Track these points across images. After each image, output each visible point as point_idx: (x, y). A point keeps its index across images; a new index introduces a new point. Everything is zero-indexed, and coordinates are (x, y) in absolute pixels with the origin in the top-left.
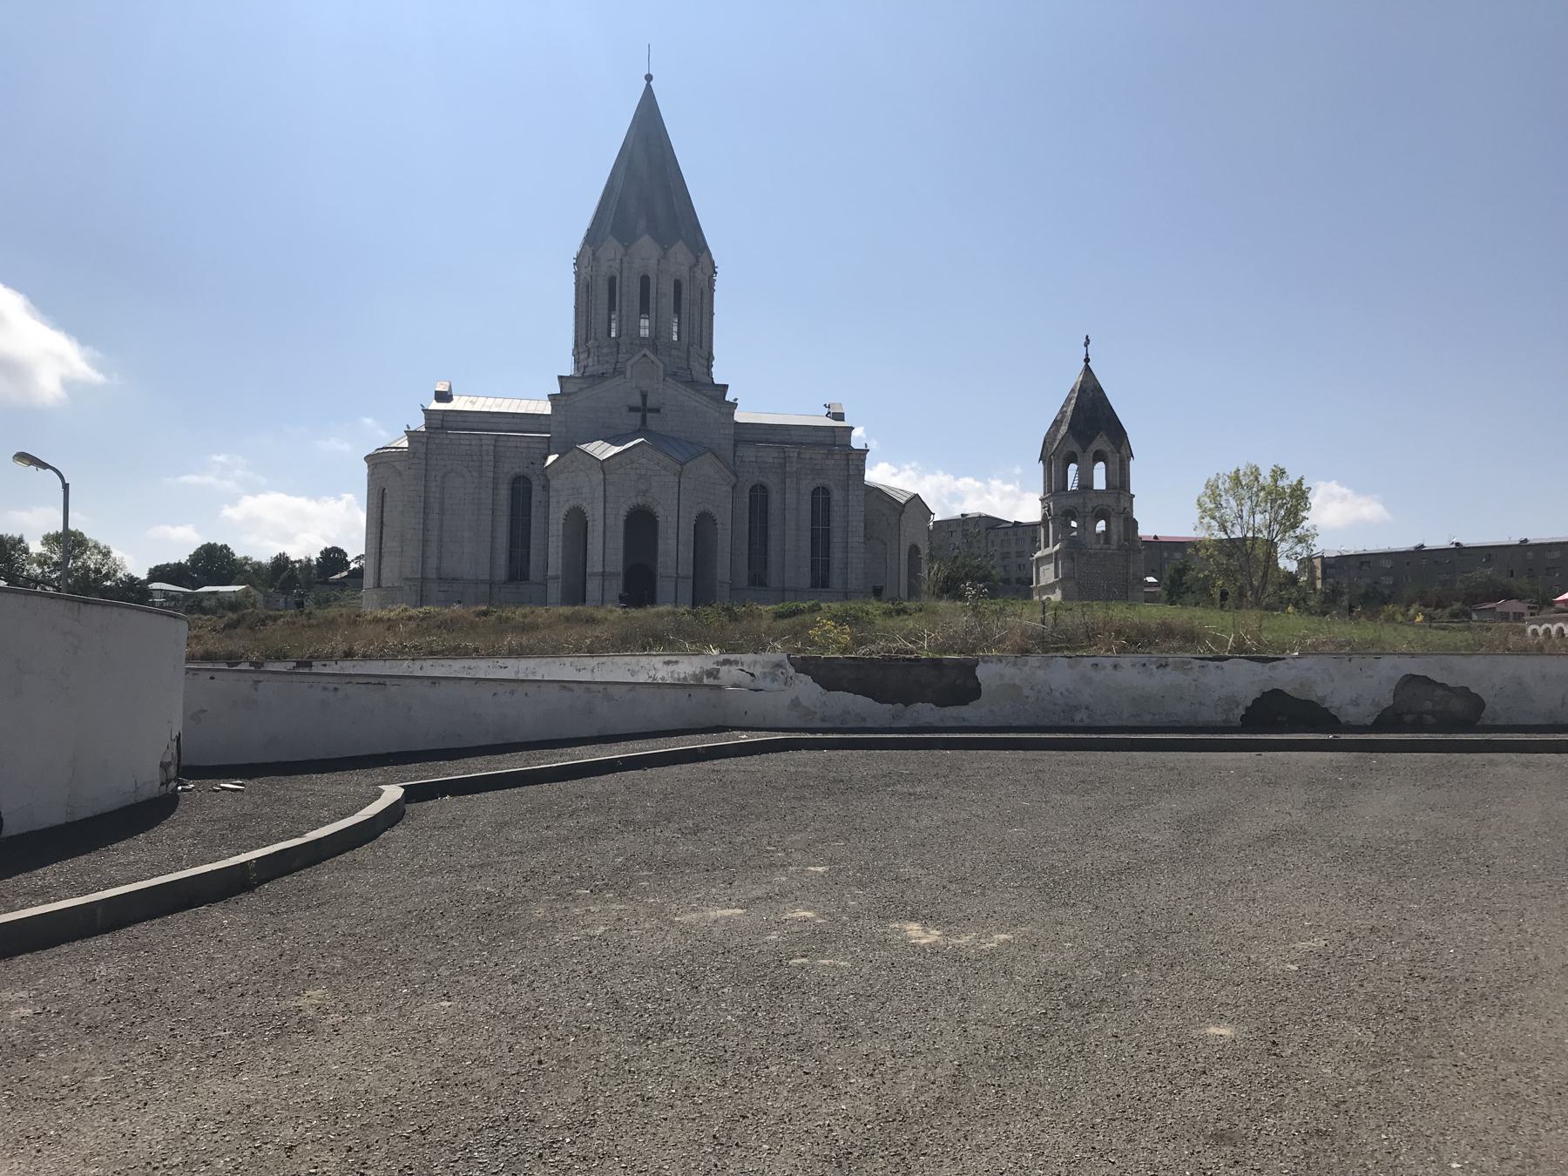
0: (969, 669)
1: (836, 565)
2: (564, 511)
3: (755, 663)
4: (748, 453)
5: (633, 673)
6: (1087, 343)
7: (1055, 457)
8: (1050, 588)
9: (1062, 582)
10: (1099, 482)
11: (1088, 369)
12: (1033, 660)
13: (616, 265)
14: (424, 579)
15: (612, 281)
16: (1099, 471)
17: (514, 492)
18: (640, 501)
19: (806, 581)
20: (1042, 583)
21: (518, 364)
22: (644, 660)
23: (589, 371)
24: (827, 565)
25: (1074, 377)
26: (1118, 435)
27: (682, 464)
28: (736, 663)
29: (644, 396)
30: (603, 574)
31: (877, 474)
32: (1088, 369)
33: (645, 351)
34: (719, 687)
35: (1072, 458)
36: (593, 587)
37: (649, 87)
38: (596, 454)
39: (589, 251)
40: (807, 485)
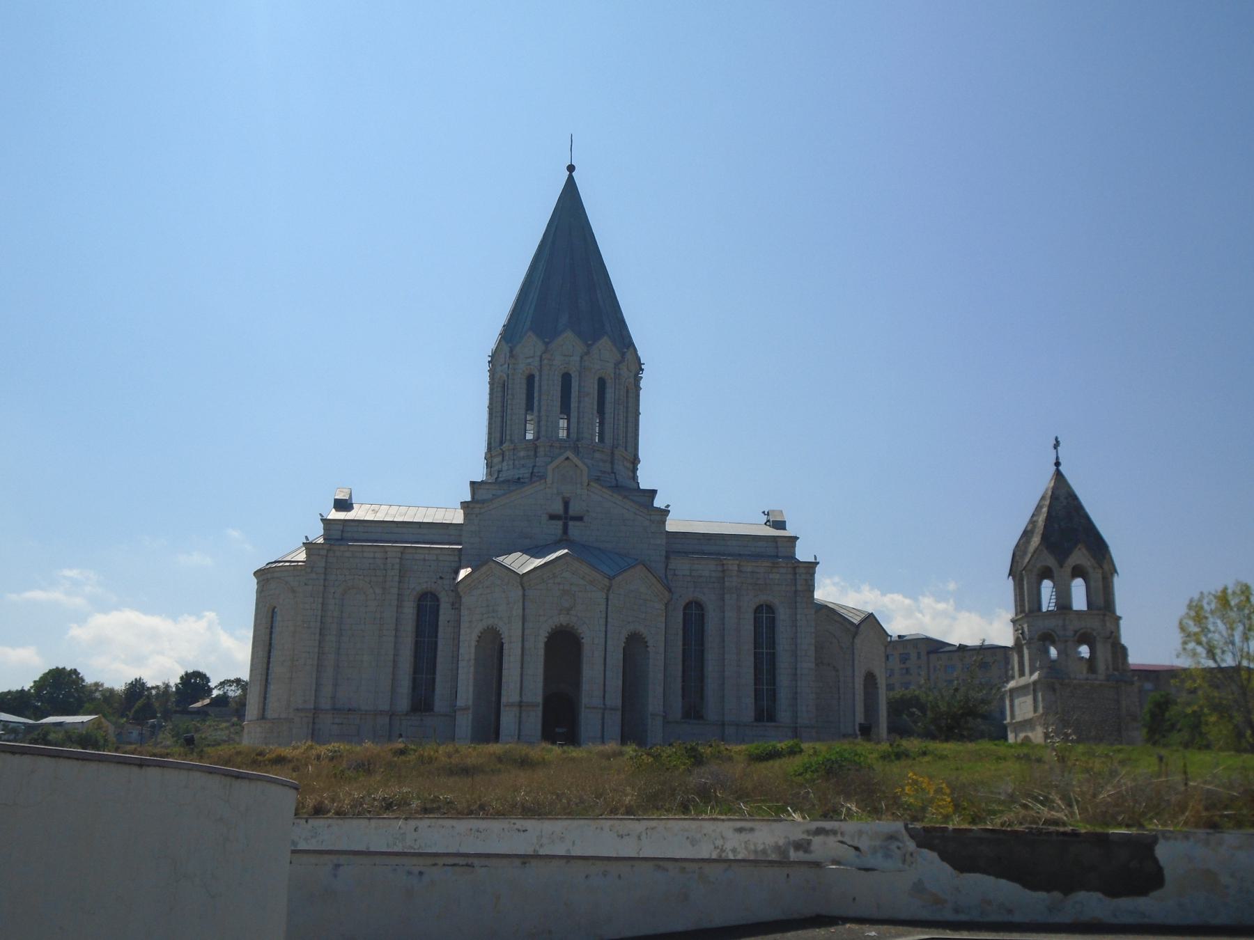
0: (1145, 847)
1: (783, 695)
3: (860, 833)
4: (681, 566)
5: (694, 842)
6: (1057, 445)
7: (1025, 572)
8: (1027, 724)
10: (1079, 601)
11: (1059, 475)
12: (1231, 837)
13: (537, 363)
14: (317, 710)
15: (530, 379)
18: (563, 620)
19: (749, 714)
20: (1018, 719)
22: (708, 827)
23: (503, 476)
25: (1044, 482)
26: (1098, 547)
27: (611, 578)
28: (834, 832)
29: (566, 504)
30: (520, 705)
31: (826, 591)
32: (1059, 475)
33: (569, 454)
34: (817, 865)
35: (1047, 573)
36: (508, 719)
38: (514, 567)
39: (506, 348)
40: (750, 602)
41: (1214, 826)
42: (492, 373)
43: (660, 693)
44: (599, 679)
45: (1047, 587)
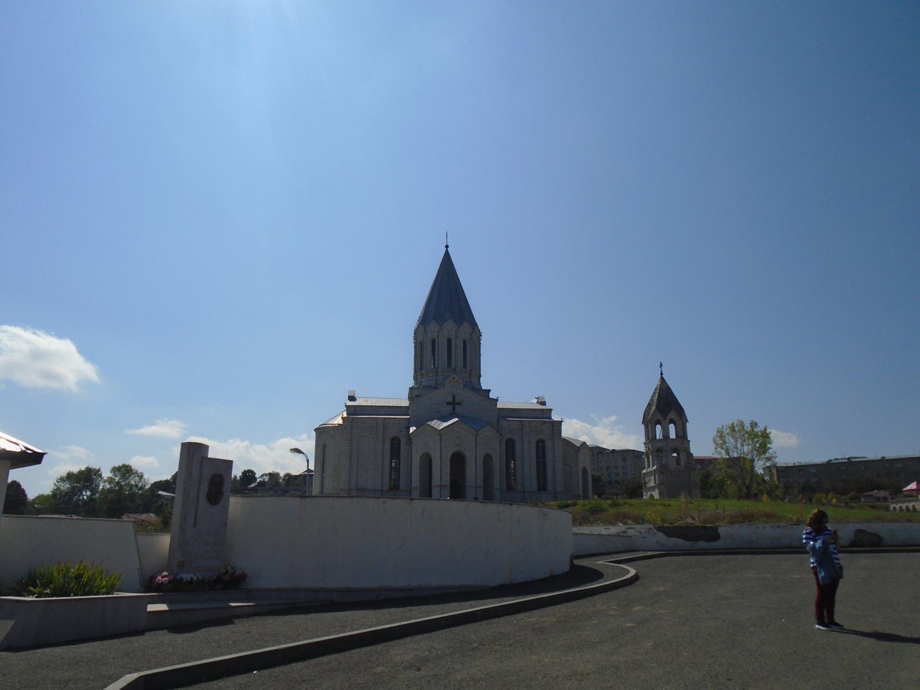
0: (715, 529)
2: (420, 455)
6: (661, 365)
7: (649, 422)
9: (659, 486)
10: (673, 435)
11: (662, 379)
12: (737, 526)
14: (350, 490)
15: (433, 341)
16: (672, 428)
17: (392, 444)
18: (458, 449)
19: (535, 487)
21: (390, 382)
23: (423, 384)
24: (545, 479)
25: (656, 382)
29: (454, 397)
30: (441, 486)
32: (662, 379)
34: (630, 537)
35: (659, 422)
36: (435, 492)
37: (447, 251)
38: (436, 426)
41: (732, 523)
42: (415, 338)
43: (497, 481)
44: (473, 473)
45: (658, 427)
